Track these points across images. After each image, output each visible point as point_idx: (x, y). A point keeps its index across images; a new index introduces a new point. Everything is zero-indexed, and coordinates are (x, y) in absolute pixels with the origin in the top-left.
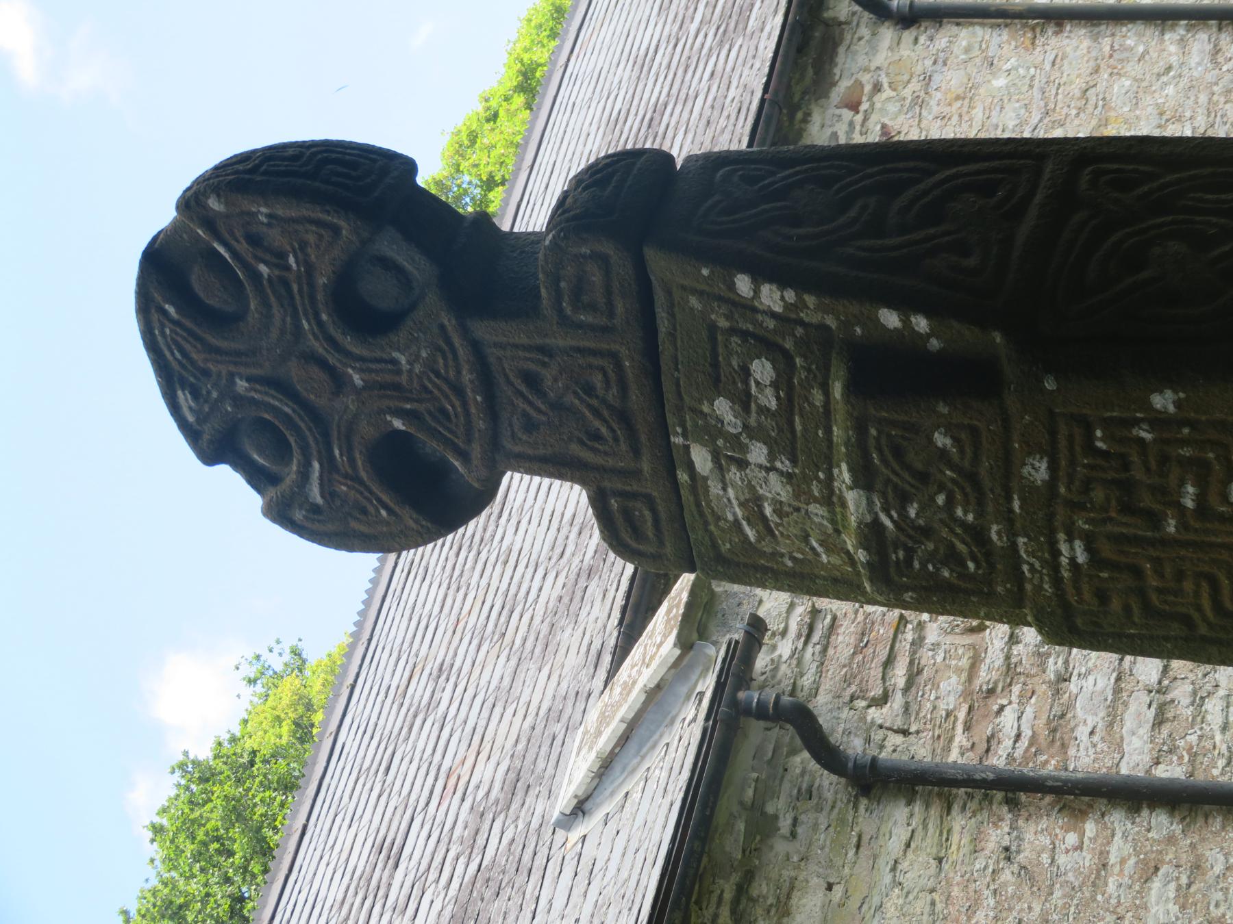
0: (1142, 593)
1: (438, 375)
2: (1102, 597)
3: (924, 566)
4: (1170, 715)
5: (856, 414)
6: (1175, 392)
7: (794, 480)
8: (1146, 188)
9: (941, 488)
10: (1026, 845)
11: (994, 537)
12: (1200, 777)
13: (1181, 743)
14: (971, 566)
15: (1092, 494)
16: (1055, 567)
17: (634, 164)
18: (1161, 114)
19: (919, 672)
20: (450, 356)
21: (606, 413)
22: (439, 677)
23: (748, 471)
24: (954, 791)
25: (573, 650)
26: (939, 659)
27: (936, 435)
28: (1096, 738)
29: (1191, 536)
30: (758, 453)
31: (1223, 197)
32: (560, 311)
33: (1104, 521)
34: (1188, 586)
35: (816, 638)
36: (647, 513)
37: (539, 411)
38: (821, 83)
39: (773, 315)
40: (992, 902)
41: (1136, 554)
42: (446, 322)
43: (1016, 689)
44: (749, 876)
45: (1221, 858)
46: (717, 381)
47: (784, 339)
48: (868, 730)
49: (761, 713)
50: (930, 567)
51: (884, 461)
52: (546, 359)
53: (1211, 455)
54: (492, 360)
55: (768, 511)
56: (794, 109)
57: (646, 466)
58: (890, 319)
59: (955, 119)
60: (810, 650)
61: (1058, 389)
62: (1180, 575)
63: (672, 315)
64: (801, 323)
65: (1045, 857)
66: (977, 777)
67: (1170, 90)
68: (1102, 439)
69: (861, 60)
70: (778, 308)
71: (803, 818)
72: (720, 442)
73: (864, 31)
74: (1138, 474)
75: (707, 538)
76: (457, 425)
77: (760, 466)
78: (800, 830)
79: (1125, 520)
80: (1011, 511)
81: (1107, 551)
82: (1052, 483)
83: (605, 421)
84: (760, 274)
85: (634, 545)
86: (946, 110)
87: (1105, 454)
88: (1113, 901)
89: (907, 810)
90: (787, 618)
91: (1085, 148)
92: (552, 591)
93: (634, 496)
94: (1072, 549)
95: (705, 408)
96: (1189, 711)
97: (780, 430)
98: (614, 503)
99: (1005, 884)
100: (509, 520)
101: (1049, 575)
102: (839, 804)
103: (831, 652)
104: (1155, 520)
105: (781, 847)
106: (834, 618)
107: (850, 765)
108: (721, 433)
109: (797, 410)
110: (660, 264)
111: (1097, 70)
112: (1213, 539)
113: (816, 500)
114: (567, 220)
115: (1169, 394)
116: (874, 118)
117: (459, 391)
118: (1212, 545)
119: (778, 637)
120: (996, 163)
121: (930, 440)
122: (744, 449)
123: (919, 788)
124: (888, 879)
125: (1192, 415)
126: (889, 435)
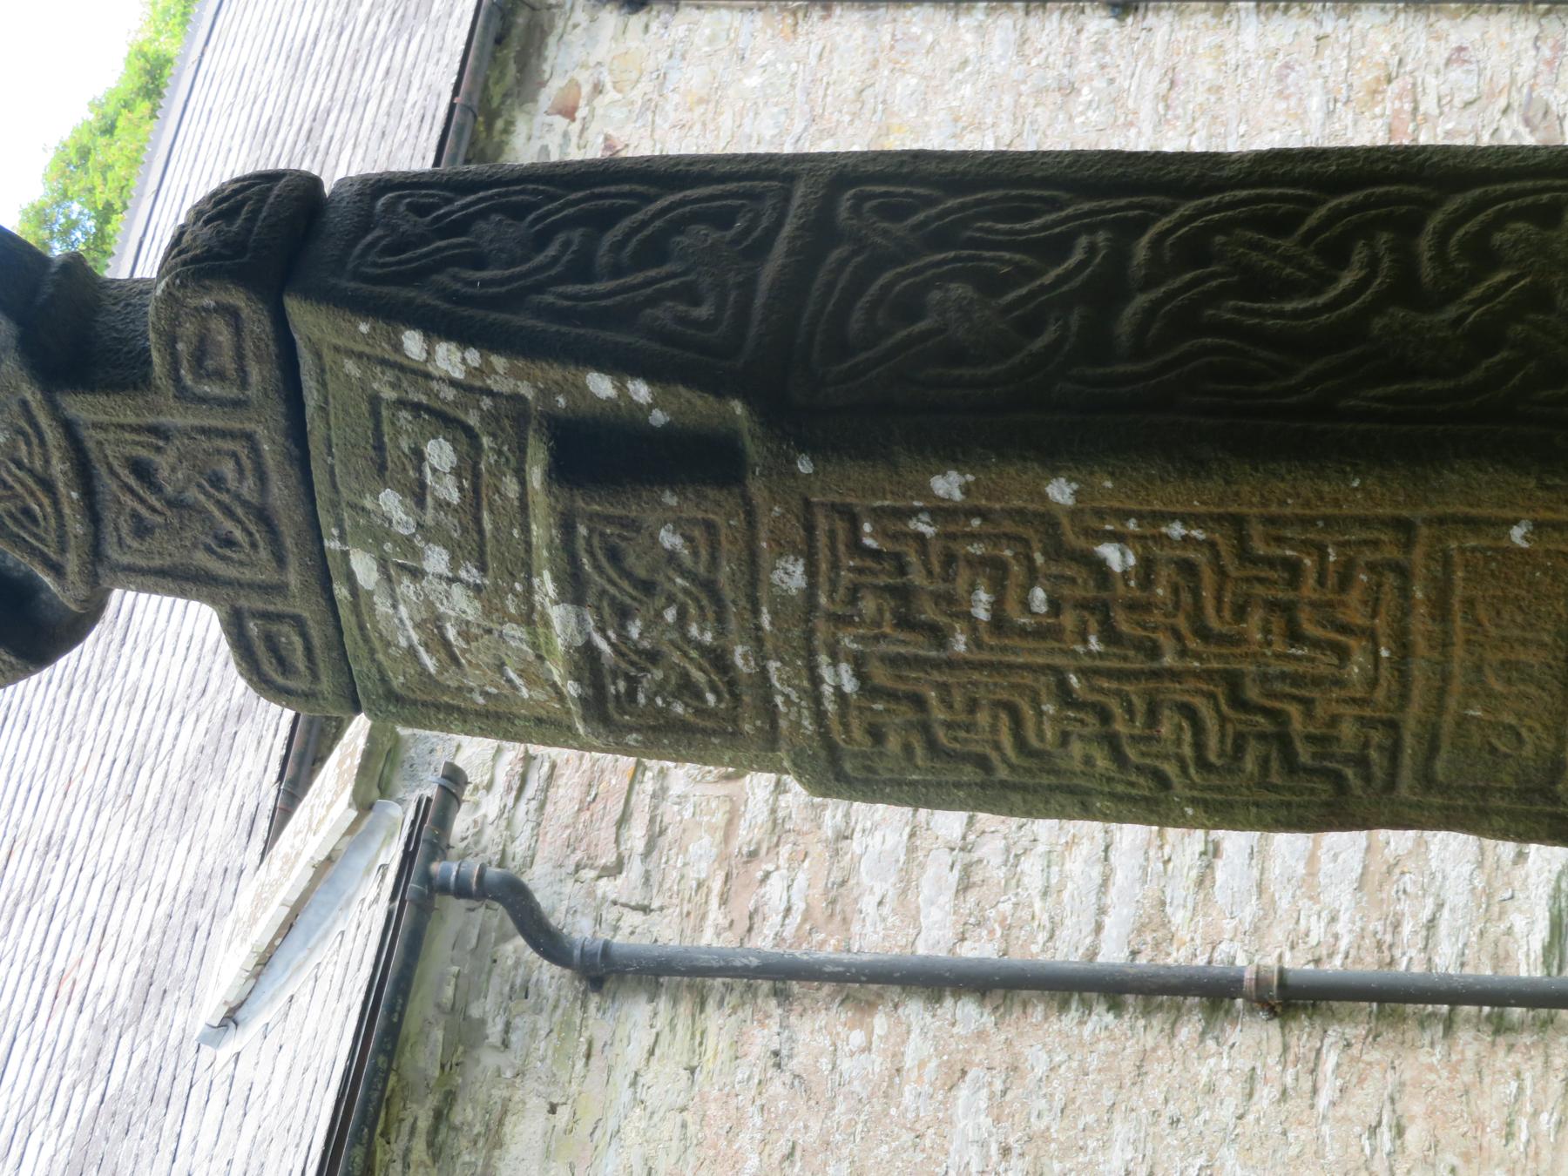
0: (925, 728)
1: (20, 465)
2: (876, 734)
3: (651, 700)
4: (976, 878)
5: (560, 507)
6: (963, 474)
7: (484, 595)
8: (921, 216)
9: (671, 599)
10: (799, 1048)
11: (739, 662)
12: (1017, 956)
13: (992, 913)
14: (711, 698)
15: (861, 604)
16: (817, 699)
17: (270, 189)
18: (956, 120)
19: (662, 832)
20: (35, 441)
21: (239, 511)
22: (47, 853)
23: (424, 583)
24: (709, 981)
25: (220, 815)
26: (687, 815)
27: (663, 533)
28: (886, 910)
29: (985, 656)
30: (436, 560)
31: (1018, 226)
32: (177, 380)
33: (877, 638)
34: (983, 718)
35: (530, 791)
36: (297, 640)
37: (154, 510)
38: (527, 82)
39: (453, 383)
40: (758, 1120)
41: (917, 679)
42: (29, 396)
43: (785, 850)
44: (450, 1098)
45: (1044, 1056)
46: (382, 468)
47: (467, 413)
48: (598, 908)
49: (461, 890)
50: (659, 701)
51: (598, 567)
52: (161, 443)
53: (1008, 553)
54: (90, 445)
55: (451, 634)
56: (491, 116)
57: (293, 578)
58: (601, 385)
59: (697, 128)
60: (522, 806)
61: (816, 473)
62: (973, 706)
63: (323, 384)
64: (490, 393)
65: (825, 1063)
66: (738, 963)
67: (967, 90)
68: (871, 535)
69: (578, 54)
70: (458, 374)
71: (517, 1021)
72: (388, 547)
73: (580, 16)
74: (917, 577)
75: (374, 670)
76: (46, 530)
77: (440, 577)
78: (514, 1038)
79: (902, 636)
80: (759, 628)
81: (881, 676)
83: (239, 521)
84: (437, 327)
85: (280, 680)
86: (686, 116)
87: (876, 554)
88: (911, 1115)
89: (649, 1008)
90: (493, 767)
91: (845, 166)
92: (191, 739)
93: (279, 617)
94: (837, 674)
95: (368, 503)
96: (1002, 873)
97: (465, 530)
98: (253, 628)
99: (774, 1098)
100: (134, 649)
101: (809, 708)
102: (563, 1003)
103: (549, 808)
104: (939, 636)
105: (489, 1059)
106: (553, 766)
107: (577, 953)
108: (389, 534)
109: (485, 503)
110: (305, 318)
111: (874, 65)
112: (1011, 658)
113: (512, 619)
114: (185, 263)
115: (954, 476)
116: (594, 127)
117: (48, 485)
118: (1010, 666)
119: (482, 792)
120: (731, 186)
121: (654, 538)
122: (417, 554)
123: (664, 980)
124: (626, 1095)
125: (983, 502)
126: (602, 534)
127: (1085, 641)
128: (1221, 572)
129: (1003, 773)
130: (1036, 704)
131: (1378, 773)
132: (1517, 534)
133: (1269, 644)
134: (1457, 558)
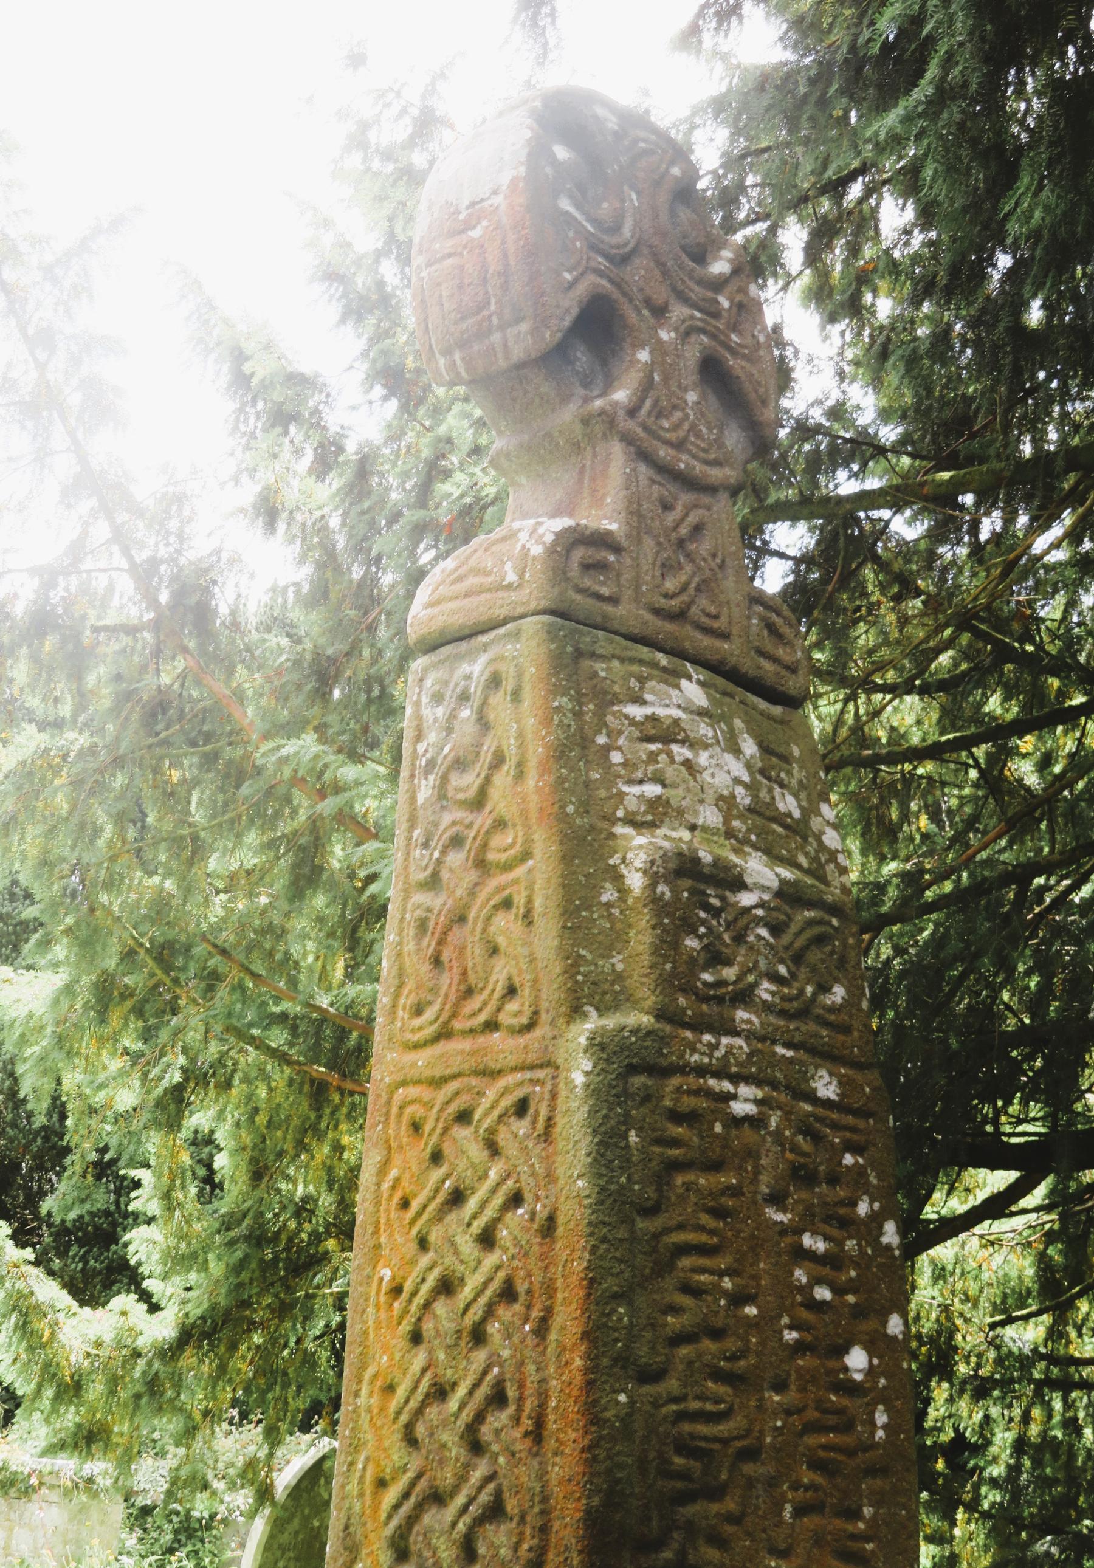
14: (707, 977)
16: (718, 1075)
80: (774, 1042)
82: (811, 1097)
94: (746, 1100)
101: (710, 1064)
127: (791, 1327)
128: (851, 1452)
129: (641, 1224)
130: (730, 1272)
133: (795, 1486)
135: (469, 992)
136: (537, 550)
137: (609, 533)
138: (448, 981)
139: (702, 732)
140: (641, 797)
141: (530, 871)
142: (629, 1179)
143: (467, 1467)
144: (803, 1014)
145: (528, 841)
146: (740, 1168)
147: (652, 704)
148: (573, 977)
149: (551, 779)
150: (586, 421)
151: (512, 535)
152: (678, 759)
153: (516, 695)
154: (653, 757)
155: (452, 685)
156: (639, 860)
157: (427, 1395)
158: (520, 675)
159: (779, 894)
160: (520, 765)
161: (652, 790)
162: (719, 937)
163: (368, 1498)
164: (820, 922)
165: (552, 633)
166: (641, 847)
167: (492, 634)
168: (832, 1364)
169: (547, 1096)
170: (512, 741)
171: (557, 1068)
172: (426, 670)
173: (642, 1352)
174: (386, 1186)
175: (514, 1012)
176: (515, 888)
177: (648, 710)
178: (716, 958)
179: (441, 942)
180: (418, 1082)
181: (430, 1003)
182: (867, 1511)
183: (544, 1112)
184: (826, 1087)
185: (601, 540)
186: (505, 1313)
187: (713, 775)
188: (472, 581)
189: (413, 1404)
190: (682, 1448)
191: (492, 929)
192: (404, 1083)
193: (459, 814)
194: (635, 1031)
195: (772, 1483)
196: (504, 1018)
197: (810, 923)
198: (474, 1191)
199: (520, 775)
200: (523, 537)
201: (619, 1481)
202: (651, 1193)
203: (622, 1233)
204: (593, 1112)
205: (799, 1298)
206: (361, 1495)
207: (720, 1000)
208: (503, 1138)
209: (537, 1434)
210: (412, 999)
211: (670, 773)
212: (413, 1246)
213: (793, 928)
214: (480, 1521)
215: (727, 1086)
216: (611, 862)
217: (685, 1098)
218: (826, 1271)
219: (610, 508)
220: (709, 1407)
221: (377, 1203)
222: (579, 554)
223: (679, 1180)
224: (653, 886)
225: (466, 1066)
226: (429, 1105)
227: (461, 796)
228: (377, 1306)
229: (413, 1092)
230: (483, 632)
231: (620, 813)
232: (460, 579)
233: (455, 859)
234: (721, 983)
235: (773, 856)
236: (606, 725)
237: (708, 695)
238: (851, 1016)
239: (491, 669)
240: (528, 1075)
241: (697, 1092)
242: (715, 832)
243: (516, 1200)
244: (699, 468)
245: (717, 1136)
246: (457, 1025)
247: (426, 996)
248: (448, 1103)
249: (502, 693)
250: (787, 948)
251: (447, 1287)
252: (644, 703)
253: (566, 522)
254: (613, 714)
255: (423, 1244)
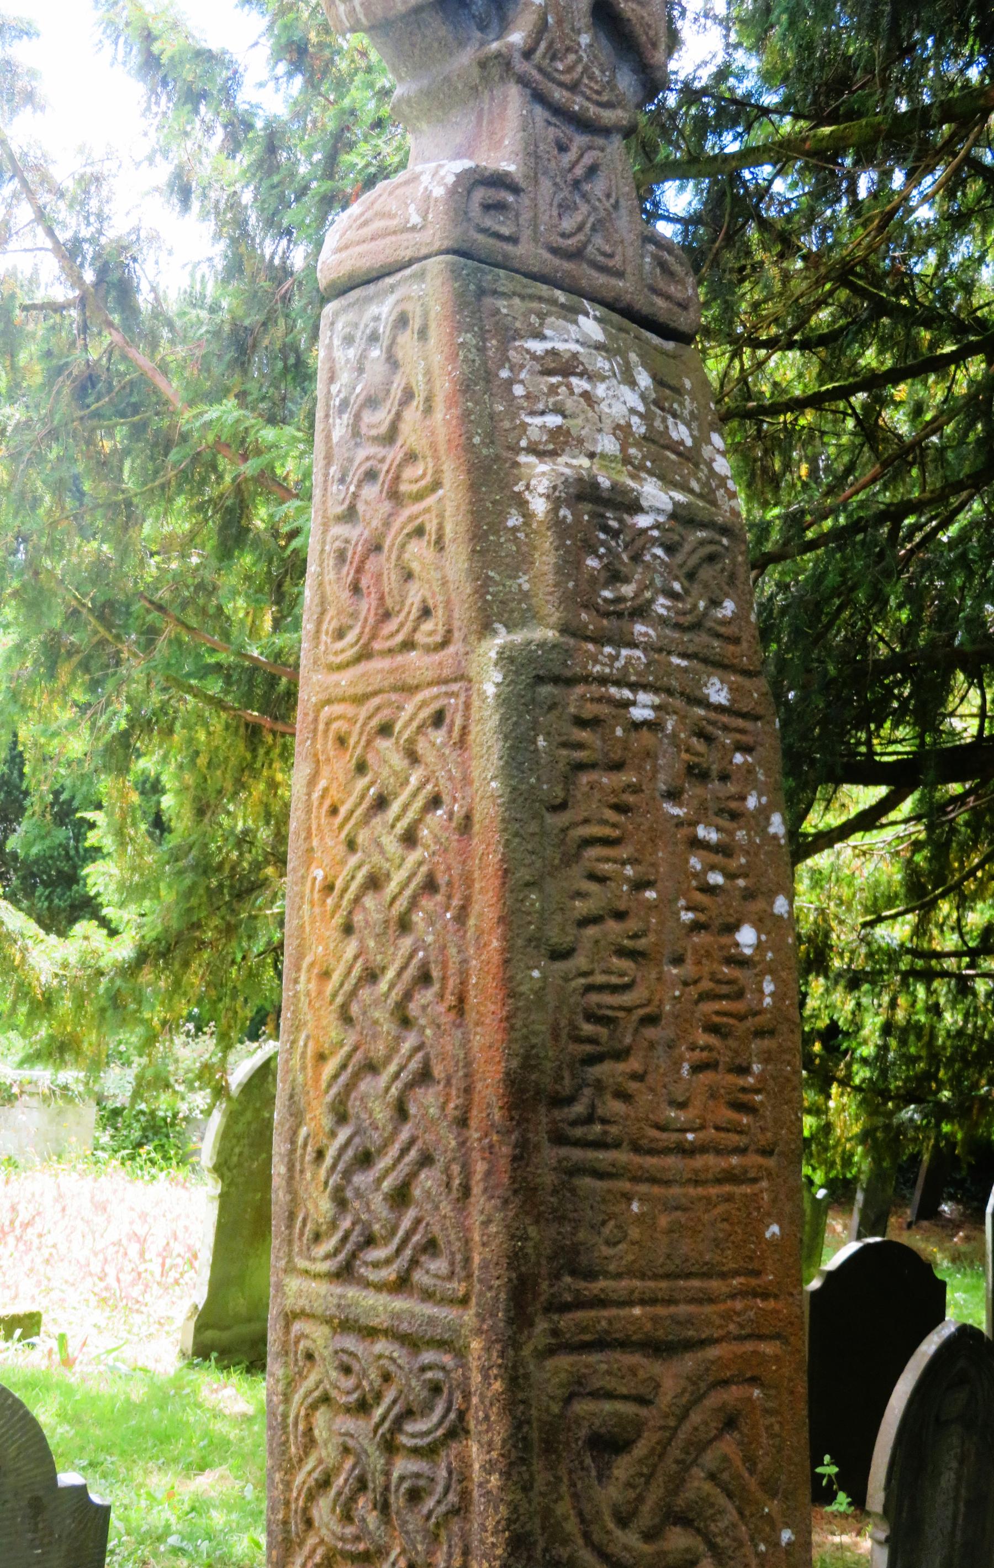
14: (607, 594)
16: (618, 683)
80: (669, 653)
82: (703, 702)
94: (645, 706)
127: (688, 909)
128: (741, 1018)
130: (633, 861)
131: (579, 1132)
132: (775, 1229)
133: (692, 1048)
134: (757, 1187)
135: (387, 615)
136: (439, 191)
137: (507, 174)
138: (367, 606)
139: (599, 365)
140: (544, 426)
141: (440, 500)
142: (538, 779)
143: (398, 1039)
144: (696, 626)
145: (438, 472)
146: (640, 768)
147: (552, 339)
148: (482, 597)
149: (456, 412)
150: (483, 65)
151: (415, 178)
152: (577, 391)
153: (423, 334)
154: (553, 389)
155: (362, 326)
156: (542, 486)
157: (360, 979)
158: (426, 315)
159: (673, 516)
160: (428, 400)
161: (553, 421)
162: (618, 556)
163: (310, 1072)
164: (711, 542)
165: (455, 273)
166: (544, 474)
167: (398, 276)
168: (724, 940)
169: (461, 707)
170: (420, 377)
171: (470, 681)
172: (336, 314)
173: (555, 935)
174: (316, 795)
175: (430, 630)
176: (427, 516)
177: (548, 345)
178: (615, 576)
179: (359, 570)
180: (342, 700)
181: (350, 627)
182: (756, 1068)
183: (458, 722)
184: (718, 693)
185: (498, 181)
186: (428, 903)
187: (610, 406)
188: (378, 225)
189: (347, 987)
190: (591, 1017)
191: (406, 556)
192: (329, 702)
193: (372, 450)
194: (541, 645)
195: (671, 1046)
196: (420, 638)
197: (702, 543)
198: (396, 795)
199: (428, 410)
200: (425, 179)
201: (533, 1047)
202: (559, 792)
203: (533, 827)
204: (504, 719)
205: (694, 883)
206: (303, 1068)
207: (619, 615)
208: (422, 746)
209: (460, 1007)
210: (335, 624)
211: (569, 405)
212: (342, 848)
213: (687, 548)
214: (410, 1086)
215: (627, 694)
216: (516, 489)
217: (588, 705)
218: (718, 859)
219: (509, 149)
220: (614, 980)
221: (309, 811)
222: (480, 194)
223: (585, 779)
224: (555, 510)
225: (386, 683)
226: (353, 721)
227: (374, 432)
228: (312, 903)
229: (338, 709)
230: (389, 274)
231: (523, 443)
232: (365, 223)
233: (370, 492)
234: (619, 600)
235: (668, 482)
236: (508, 359)
237: (604, 330)
238: (740, 629)
239: (398, 309)
240: (444, 688)
241: (600, 700)
242: (613, 459)
243: (435, 802)
244: (593, 110)
245: (618, 739)
246: (377, 646)
247: (345, 620)
248: (370, 718)
249: (409, 332)
250: (681, 566)
251: (374, 883)
252: (543, 338)
253: (467, 164)
254: (516, 349)
255: (351, 845)
